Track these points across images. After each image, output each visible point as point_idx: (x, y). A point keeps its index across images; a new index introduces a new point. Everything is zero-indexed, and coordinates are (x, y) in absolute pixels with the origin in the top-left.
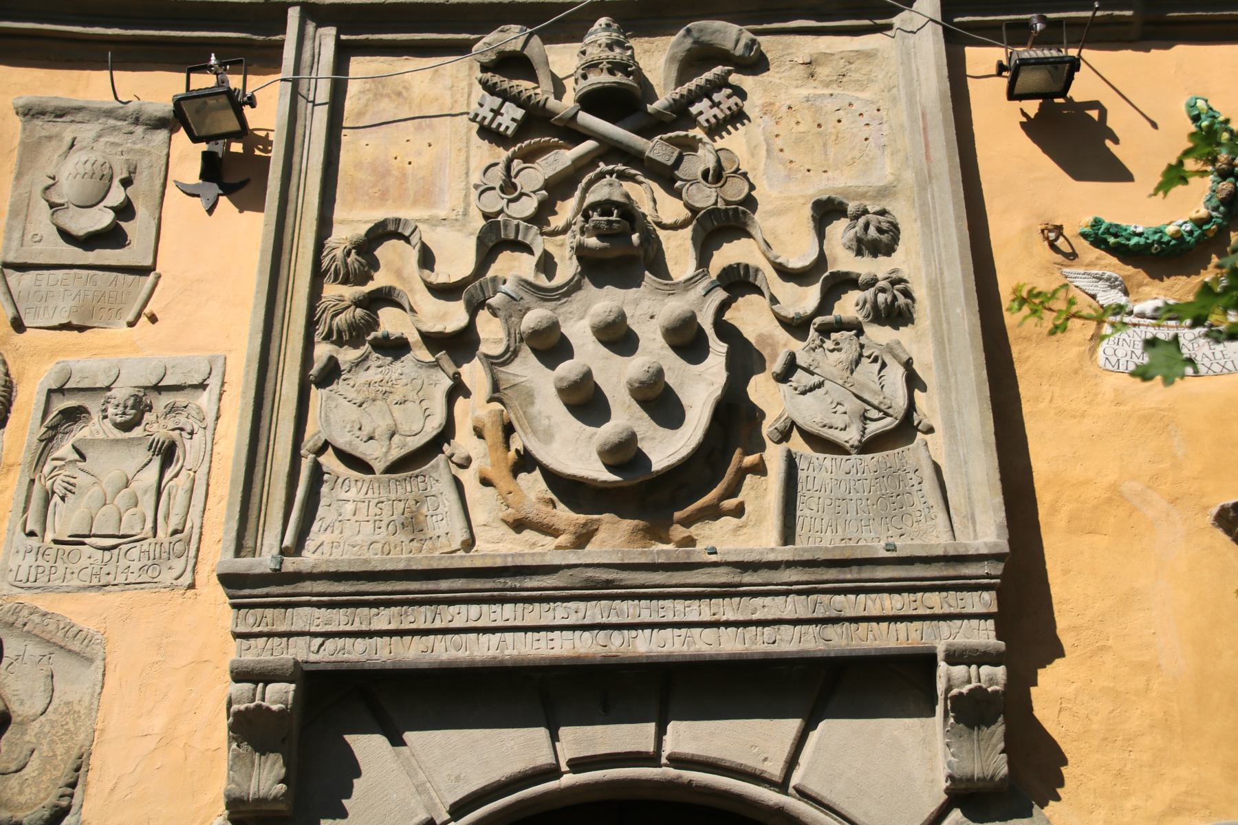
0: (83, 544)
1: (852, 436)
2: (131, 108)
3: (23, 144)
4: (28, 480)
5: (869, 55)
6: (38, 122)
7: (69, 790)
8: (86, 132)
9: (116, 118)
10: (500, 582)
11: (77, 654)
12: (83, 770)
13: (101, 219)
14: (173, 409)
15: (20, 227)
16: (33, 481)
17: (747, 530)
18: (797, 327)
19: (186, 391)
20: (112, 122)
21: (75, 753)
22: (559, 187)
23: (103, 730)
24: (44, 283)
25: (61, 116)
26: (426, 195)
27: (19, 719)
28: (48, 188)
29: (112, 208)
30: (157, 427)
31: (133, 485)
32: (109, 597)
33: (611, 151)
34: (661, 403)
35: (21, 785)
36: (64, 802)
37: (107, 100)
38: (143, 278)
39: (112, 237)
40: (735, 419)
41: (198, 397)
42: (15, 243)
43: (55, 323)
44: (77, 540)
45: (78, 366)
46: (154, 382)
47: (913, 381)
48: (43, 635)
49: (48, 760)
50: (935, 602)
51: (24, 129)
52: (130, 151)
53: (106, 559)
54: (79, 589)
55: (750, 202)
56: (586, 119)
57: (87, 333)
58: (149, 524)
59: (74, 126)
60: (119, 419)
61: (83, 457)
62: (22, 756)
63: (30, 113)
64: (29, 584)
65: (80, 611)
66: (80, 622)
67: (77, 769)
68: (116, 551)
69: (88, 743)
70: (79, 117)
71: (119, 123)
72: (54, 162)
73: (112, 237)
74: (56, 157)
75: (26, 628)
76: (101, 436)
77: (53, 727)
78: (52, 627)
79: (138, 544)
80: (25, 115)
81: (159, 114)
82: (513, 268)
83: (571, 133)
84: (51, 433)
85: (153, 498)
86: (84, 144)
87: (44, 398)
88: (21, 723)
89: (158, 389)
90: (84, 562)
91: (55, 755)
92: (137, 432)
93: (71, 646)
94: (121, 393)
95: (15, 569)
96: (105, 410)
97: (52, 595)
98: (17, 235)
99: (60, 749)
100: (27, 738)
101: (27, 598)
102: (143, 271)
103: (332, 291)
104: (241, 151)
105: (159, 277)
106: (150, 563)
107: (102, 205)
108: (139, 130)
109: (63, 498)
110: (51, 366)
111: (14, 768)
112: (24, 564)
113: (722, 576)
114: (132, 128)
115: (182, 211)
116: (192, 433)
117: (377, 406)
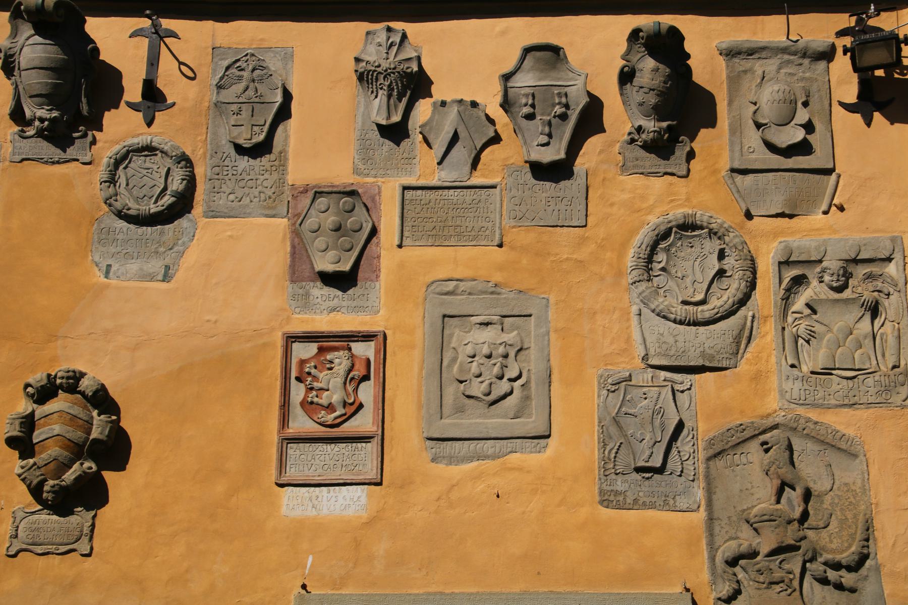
0: (831, 374)
2: (801, 44)
3: (728, 77)
4: (780, 327)
6: (736, 60)
7: (866, 543)
8: (771, 65)
9: (789, 54)
11: (845, 451)
12: (871, 530)
14: (870, 277)
15: (739, 141)
16: (784, 329)
19: (876, 263)
20: (786, 57)
21: (861, 518)
23: (877, 504)
24: (760, 184)
25: (751, 55)
27: (816, 493)
28: (755, 112)
29: (800, 125)
30: (859, 288)
31: (855, 332)
32: (858, 412)
35: (830, 536)
36: (865, 551)
37: (781, 39)
38: (826, 177)
39: (804, 148)
41: (886, 267)
42: (737, 154)
43: (774, 213)
44: (827, 372)
45: (795, 244)
46: (853, 256)
48: (818, 437)
49: (843, 522)
51: (727, 66)
52: (803, 79)
53: (851, 386)
54: (837, 406)
57: (795, 220)
58: (874, 362)
59: (761, 62)
60: (835, 285)
61: (814, 312)
62: (825, 518)
63: (731, 53)
64: (801, 402)
65: (840, 421)
66: (842, 429)
67: (868, 530)
68: (856, 380)
69: (869, 512)
70: (764, 54)
71: (792, 57)
72: (753, 91)
73: (804, 148)
74: (754, 87)
75: (805, 432)
76: (823, 296)
77: (840, 500)
78: (822, 432)
79: (871, 375)
80: (727, 55)
81: (821, 49)
84: (788, 294)
85: (872, 342)
86: (772, 76)
87: (777, 268)
88: (818, 496)
89: (856, 261)
90: (835, 387)
91: (847, 519)
92: (847, 294)
94: (832, 264)
95: (789, 391)
96: (822, 277)
97: (818, 410)
98: (737, 148)
99: (849, 515)
100: (825, 506)
101: (801, 411)
102: (828, 172)
104: (883, 75)
105: (839, 176)
106: (883, 389)
107: (793, 123)
108: (806, 61)
109: (808, 342)
110: (776, 244)
111: (823, 526)
112: (795, 388)
114: (801, 61)
115: (847, 124)
116: (888, 295)
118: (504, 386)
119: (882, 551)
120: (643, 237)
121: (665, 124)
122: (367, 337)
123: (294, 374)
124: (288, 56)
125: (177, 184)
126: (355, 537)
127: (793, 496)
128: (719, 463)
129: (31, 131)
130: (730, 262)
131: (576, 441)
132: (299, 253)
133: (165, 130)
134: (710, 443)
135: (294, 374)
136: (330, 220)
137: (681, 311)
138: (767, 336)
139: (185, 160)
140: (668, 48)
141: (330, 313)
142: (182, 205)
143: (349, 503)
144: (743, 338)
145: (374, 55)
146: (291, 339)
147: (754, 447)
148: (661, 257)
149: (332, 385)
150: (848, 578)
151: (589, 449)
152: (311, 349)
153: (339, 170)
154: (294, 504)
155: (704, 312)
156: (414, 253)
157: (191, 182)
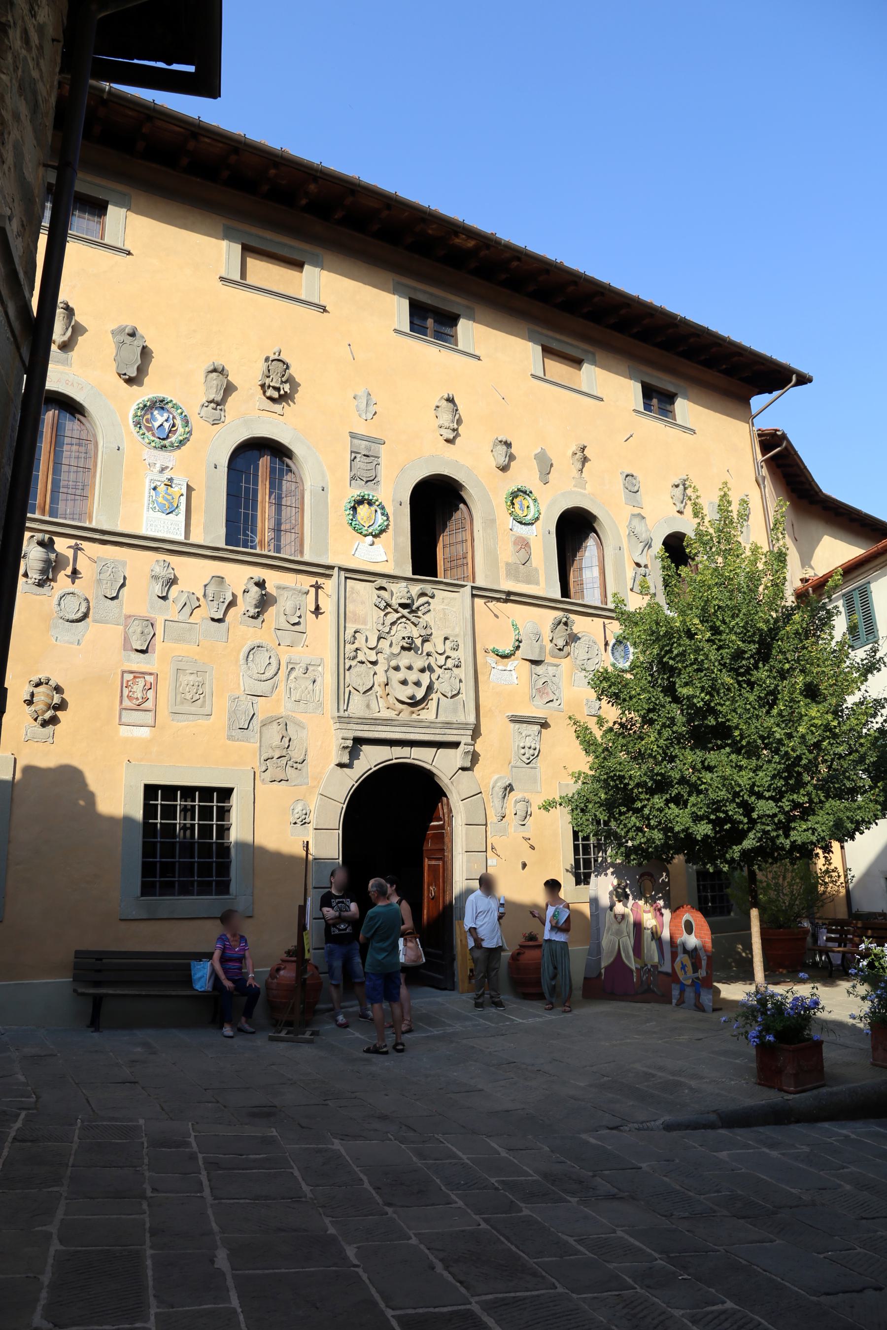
1: (449, 695)
5: (455, 599)
10: (386, 722)
13: (297, 620)
17: (428, 714)
18: (441, 667)
22: (393, 624)
26: (365, 623)
33: (403, 616)
34: (418, 684)
39: (298, 623)
40: (430, 688)
47: (461, 681)
50: (462, 732)
55: (431, 635)
56: (400, 609)
65: (300, 717)
73: (298, 623)
82: (384, 644)
83: (396, 611)
93: (300, 725)
103: (347, 646)
113: (427, 724)
117: (359, 677)
118: (197, 696)
119: (309, 759)
120: (245, 649)
121: (257, 610)
122: (151, 674)
123: (124, 685)
124: (124, 564)
125: (83, 609)
127: (286, 740)
128: (264, 728)
129: (30, 581)
130: (273, 660)
131: (220, 719)
132: (126, 640)
133: (78, 587)
134: (262, 722)
135: (124, 685)
136: (139, 630)
137: (256, 676)
138: (282, 686)
139: (86, 599)
140: (261, 584)
141: (138, 663)
142: (85, 616)
143: (144, 732)
144: (275, 687)
145: (158, 570)
146: (123, 672)
147: (275, 723)
148: (251, 656)
149: (138, 689)
150: (299, 766)
152: (131, 676)
153: (143, 611)
154: (124, 731)
155: (264, 677)
156: (168, 644)
157: (88, 608)
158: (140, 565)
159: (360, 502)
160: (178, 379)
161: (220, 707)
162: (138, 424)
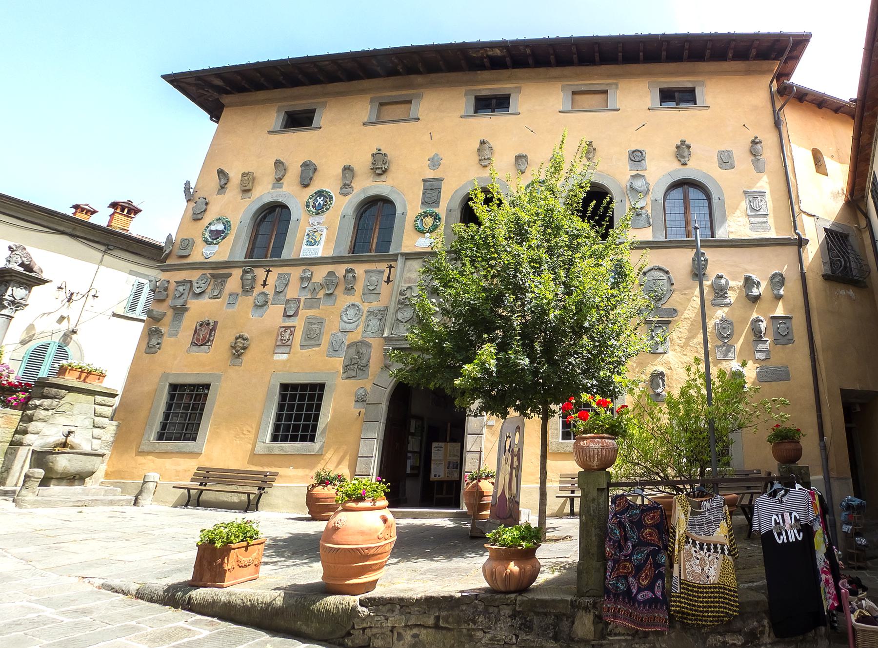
126: (284, 363)
143: (285, 357)
149: (287, 336)
151: (327, 347)
154: (277, 357)
158: (296, 273)
159: (425, 215)
160: (328, 180)
161: (325, 340)
162: (308, 206)
